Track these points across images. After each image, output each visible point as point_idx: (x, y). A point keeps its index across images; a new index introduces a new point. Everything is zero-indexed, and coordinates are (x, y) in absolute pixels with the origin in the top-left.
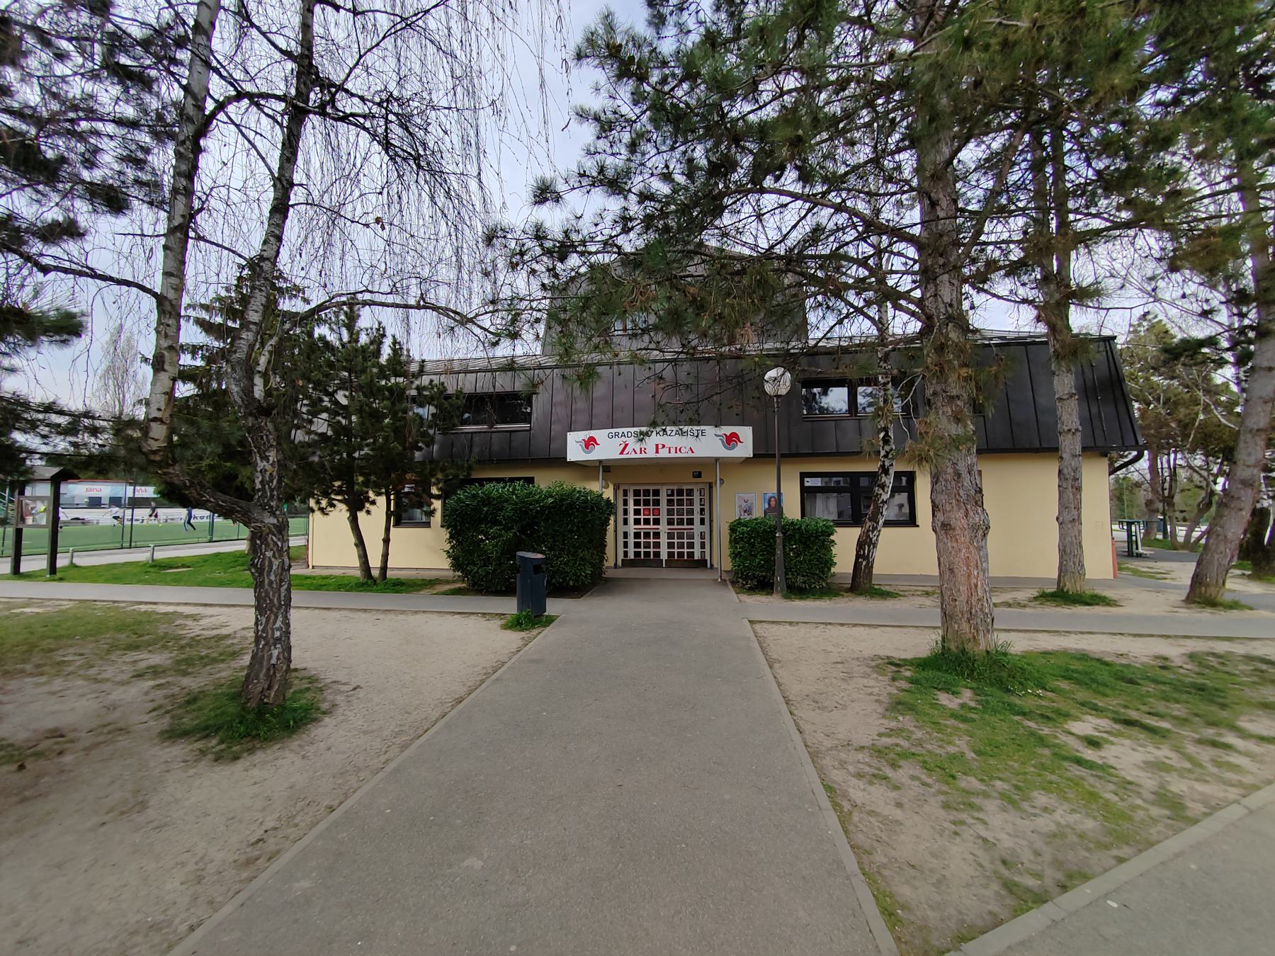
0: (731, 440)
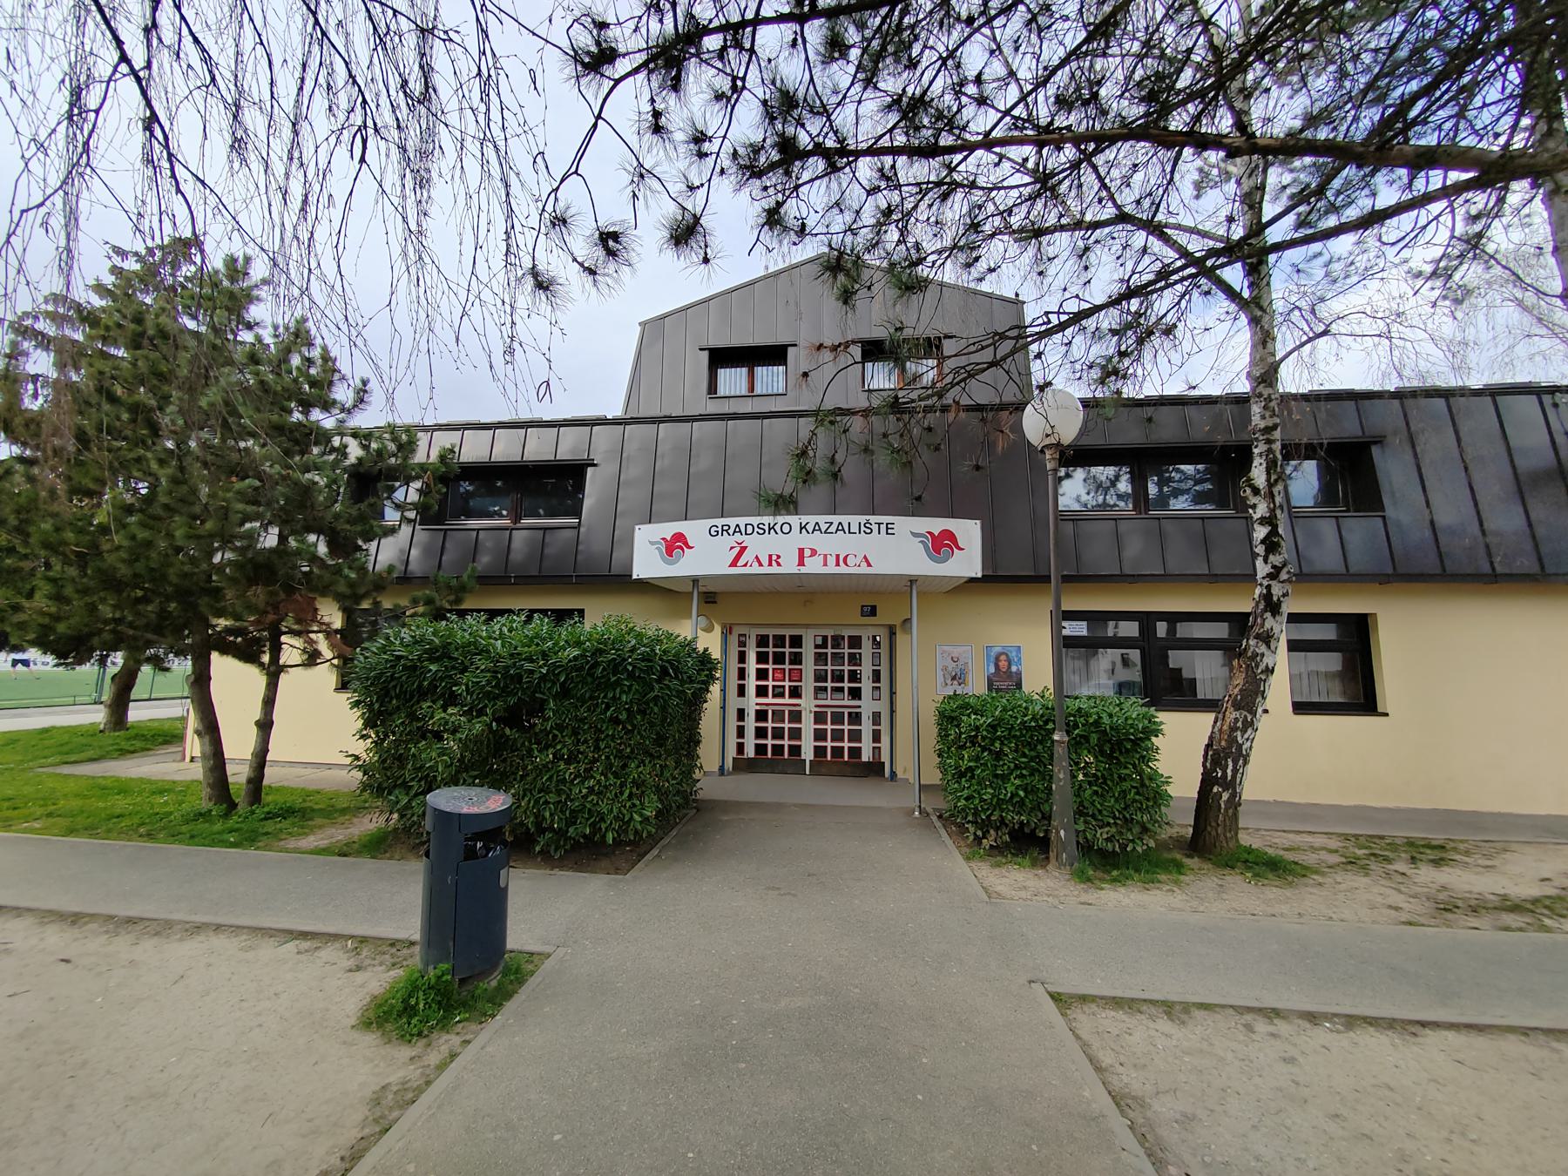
0: (942, 544)
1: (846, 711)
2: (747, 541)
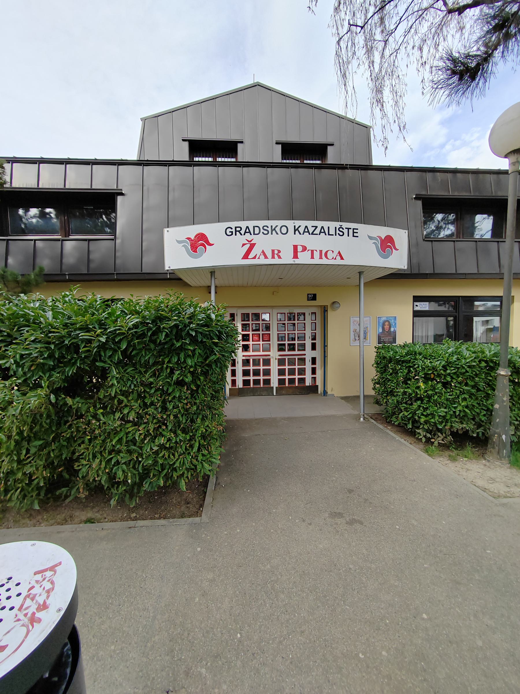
0: (387, 245)
1: (297, 357)
2: (256, 239)
